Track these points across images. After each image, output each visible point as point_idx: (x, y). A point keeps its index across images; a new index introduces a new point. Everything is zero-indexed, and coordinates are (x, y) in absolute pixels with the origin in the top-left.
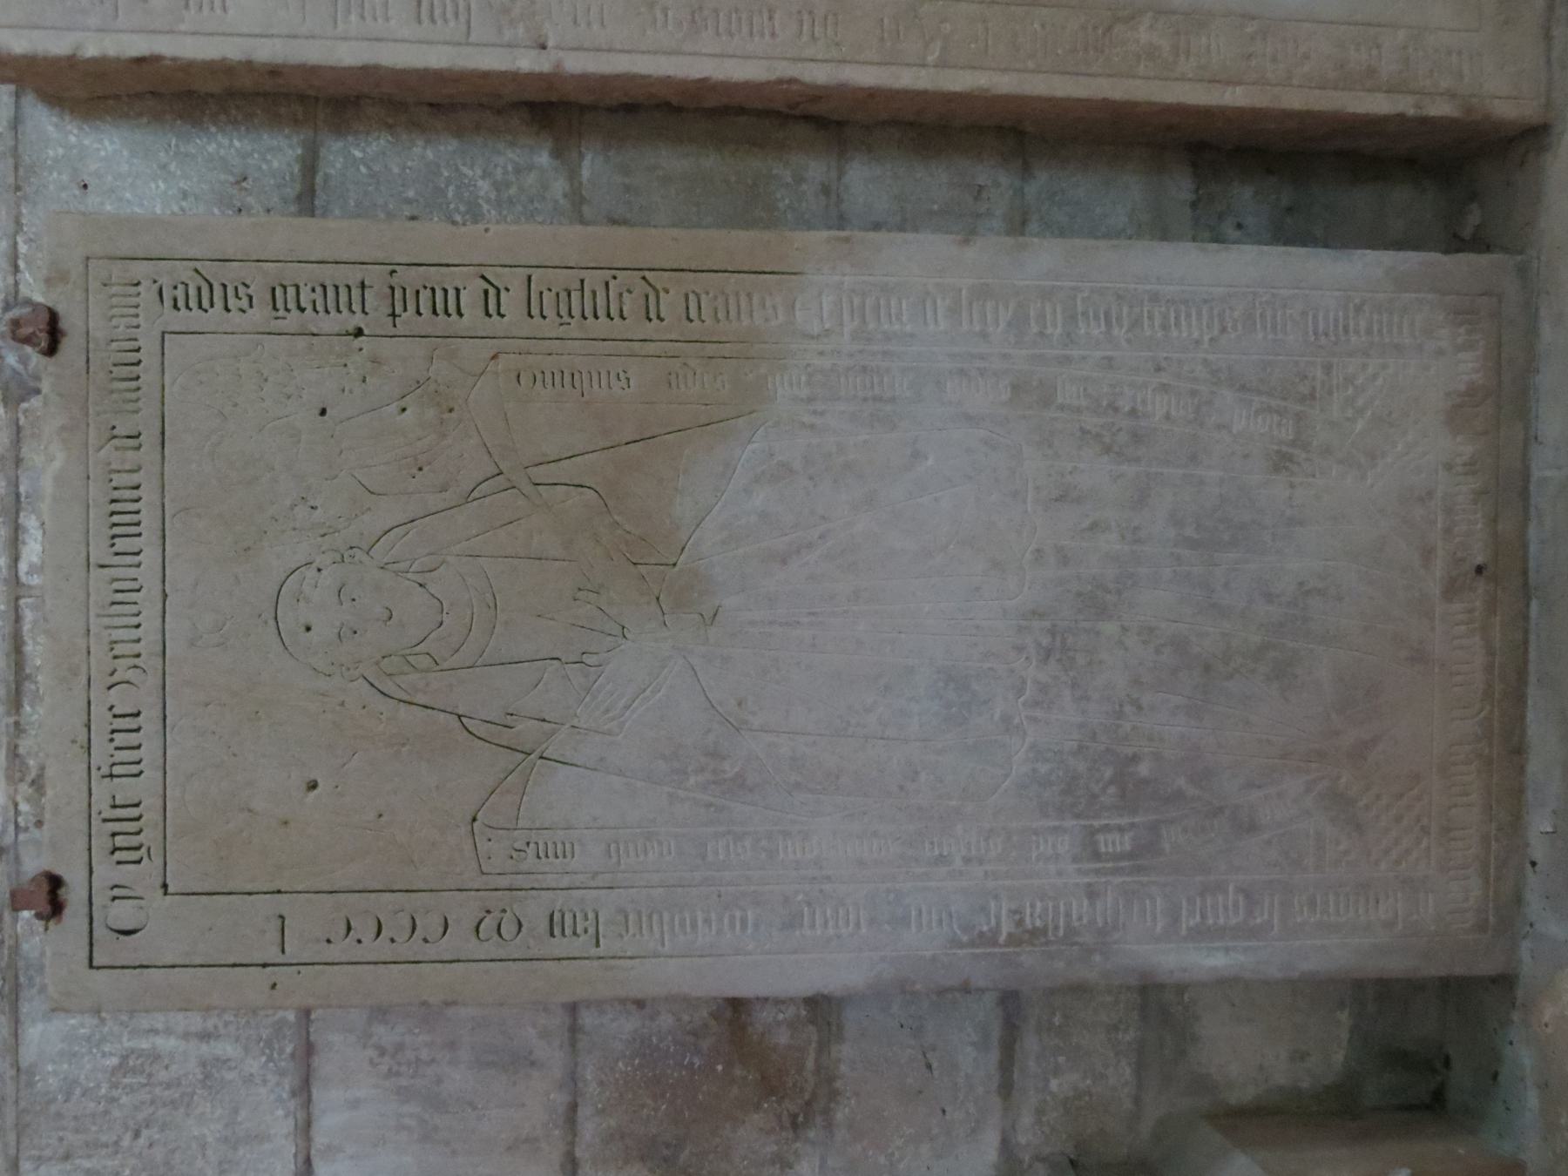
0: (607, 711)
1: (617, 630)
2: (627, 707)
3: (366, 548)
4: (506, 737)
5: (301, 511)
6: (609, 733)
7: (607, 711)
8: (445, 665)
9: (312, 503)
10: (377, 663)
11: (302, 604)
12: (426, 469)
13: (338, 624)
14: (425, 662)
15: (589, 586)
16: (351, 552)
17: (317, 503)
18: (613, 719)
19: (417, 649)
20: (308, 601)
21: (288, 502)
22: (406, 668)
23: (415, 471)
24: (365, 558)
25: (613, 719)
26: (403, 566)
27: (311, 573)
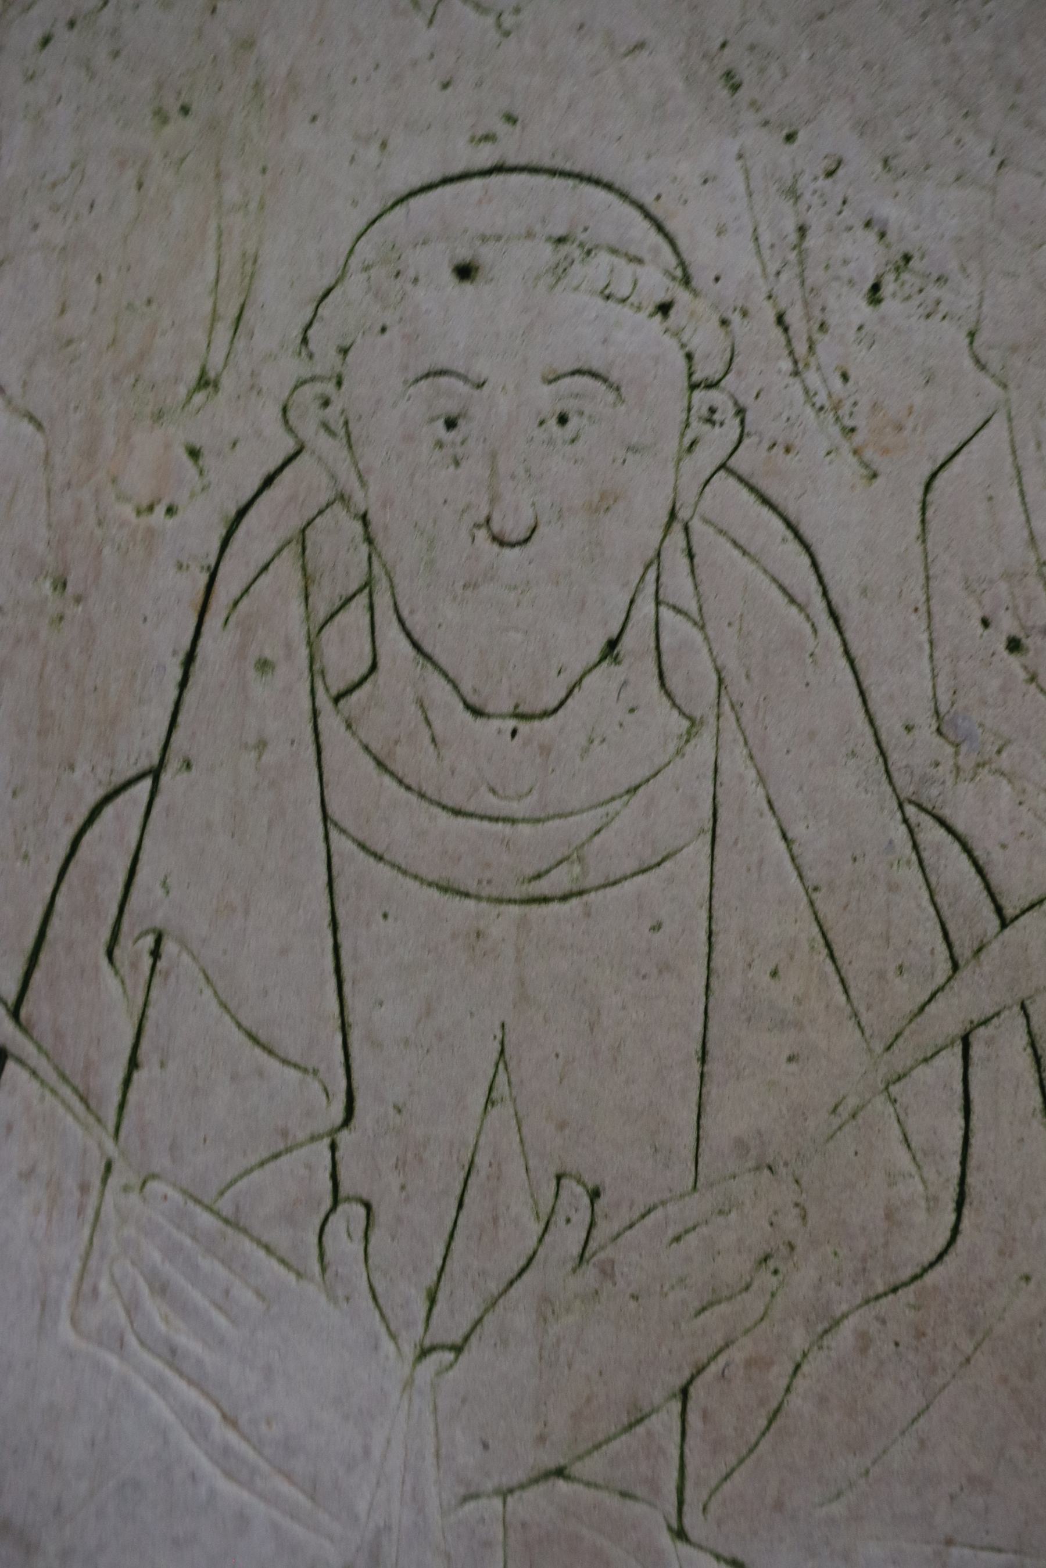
0: (162, 1289)
1: (449, 1325)
2: (172, 1355)
3: (741, 462)
4: (79, 933)
5: (866, 257)
6: (86, 1294)
7: (162, 1289)
8: (331, 722)
9: (889, 288)
10: (342, 498)
11: (547, 252)
12: (1014, 662)
13: (481, 368)
14: (344, 657)
15: (604, 1230)
16: (726, 412)
17: (890, 305)
18: (132, 1308)
19: (391, 636)
20: (560, 271)
21: (890, 211)
22: (322, 611)
23: (1007, 625)
24: (707, 457)
25: (132, 1308)
26: (675, 560)
27: (655, 283)
